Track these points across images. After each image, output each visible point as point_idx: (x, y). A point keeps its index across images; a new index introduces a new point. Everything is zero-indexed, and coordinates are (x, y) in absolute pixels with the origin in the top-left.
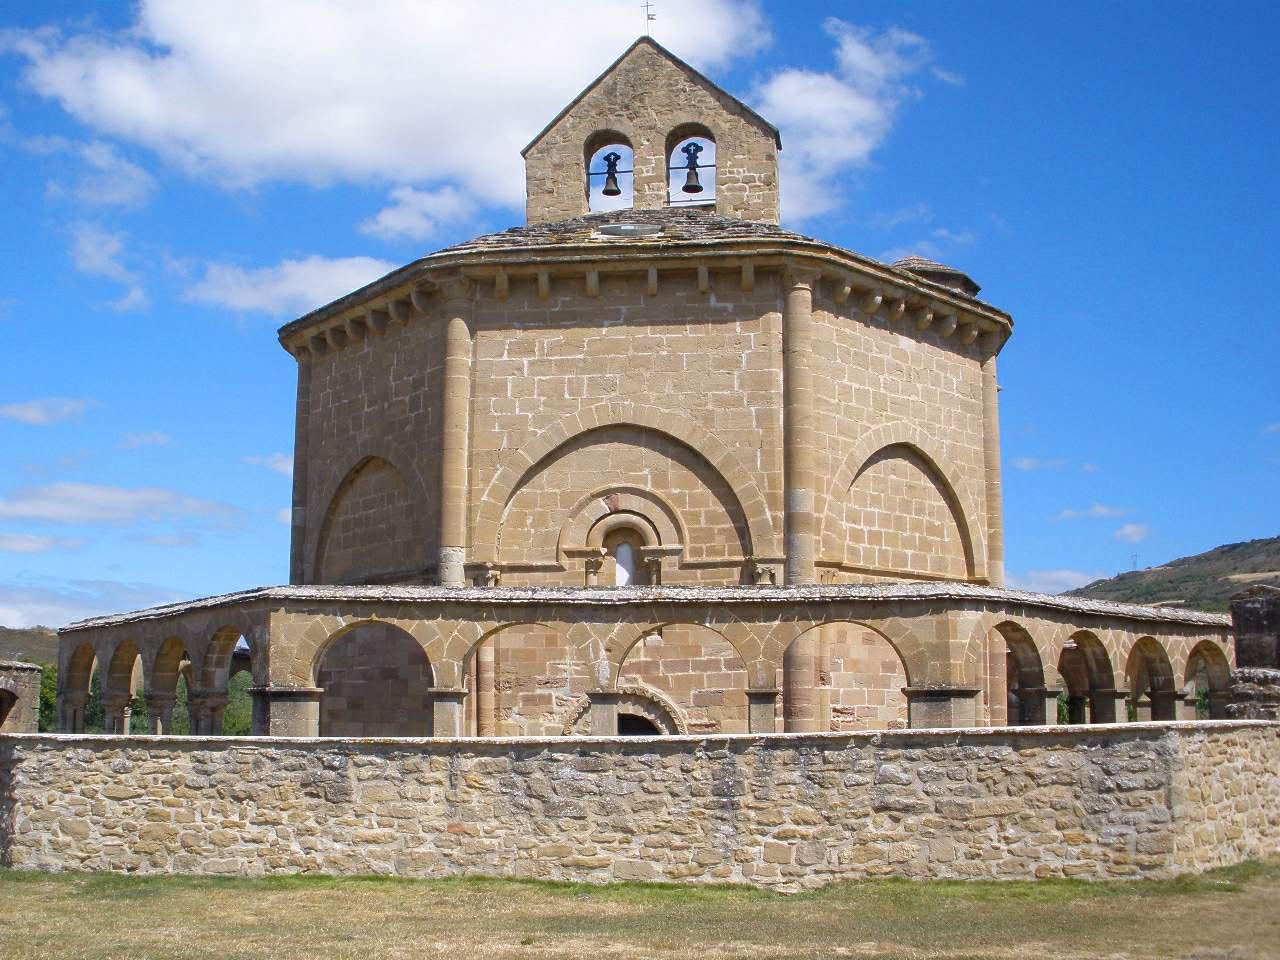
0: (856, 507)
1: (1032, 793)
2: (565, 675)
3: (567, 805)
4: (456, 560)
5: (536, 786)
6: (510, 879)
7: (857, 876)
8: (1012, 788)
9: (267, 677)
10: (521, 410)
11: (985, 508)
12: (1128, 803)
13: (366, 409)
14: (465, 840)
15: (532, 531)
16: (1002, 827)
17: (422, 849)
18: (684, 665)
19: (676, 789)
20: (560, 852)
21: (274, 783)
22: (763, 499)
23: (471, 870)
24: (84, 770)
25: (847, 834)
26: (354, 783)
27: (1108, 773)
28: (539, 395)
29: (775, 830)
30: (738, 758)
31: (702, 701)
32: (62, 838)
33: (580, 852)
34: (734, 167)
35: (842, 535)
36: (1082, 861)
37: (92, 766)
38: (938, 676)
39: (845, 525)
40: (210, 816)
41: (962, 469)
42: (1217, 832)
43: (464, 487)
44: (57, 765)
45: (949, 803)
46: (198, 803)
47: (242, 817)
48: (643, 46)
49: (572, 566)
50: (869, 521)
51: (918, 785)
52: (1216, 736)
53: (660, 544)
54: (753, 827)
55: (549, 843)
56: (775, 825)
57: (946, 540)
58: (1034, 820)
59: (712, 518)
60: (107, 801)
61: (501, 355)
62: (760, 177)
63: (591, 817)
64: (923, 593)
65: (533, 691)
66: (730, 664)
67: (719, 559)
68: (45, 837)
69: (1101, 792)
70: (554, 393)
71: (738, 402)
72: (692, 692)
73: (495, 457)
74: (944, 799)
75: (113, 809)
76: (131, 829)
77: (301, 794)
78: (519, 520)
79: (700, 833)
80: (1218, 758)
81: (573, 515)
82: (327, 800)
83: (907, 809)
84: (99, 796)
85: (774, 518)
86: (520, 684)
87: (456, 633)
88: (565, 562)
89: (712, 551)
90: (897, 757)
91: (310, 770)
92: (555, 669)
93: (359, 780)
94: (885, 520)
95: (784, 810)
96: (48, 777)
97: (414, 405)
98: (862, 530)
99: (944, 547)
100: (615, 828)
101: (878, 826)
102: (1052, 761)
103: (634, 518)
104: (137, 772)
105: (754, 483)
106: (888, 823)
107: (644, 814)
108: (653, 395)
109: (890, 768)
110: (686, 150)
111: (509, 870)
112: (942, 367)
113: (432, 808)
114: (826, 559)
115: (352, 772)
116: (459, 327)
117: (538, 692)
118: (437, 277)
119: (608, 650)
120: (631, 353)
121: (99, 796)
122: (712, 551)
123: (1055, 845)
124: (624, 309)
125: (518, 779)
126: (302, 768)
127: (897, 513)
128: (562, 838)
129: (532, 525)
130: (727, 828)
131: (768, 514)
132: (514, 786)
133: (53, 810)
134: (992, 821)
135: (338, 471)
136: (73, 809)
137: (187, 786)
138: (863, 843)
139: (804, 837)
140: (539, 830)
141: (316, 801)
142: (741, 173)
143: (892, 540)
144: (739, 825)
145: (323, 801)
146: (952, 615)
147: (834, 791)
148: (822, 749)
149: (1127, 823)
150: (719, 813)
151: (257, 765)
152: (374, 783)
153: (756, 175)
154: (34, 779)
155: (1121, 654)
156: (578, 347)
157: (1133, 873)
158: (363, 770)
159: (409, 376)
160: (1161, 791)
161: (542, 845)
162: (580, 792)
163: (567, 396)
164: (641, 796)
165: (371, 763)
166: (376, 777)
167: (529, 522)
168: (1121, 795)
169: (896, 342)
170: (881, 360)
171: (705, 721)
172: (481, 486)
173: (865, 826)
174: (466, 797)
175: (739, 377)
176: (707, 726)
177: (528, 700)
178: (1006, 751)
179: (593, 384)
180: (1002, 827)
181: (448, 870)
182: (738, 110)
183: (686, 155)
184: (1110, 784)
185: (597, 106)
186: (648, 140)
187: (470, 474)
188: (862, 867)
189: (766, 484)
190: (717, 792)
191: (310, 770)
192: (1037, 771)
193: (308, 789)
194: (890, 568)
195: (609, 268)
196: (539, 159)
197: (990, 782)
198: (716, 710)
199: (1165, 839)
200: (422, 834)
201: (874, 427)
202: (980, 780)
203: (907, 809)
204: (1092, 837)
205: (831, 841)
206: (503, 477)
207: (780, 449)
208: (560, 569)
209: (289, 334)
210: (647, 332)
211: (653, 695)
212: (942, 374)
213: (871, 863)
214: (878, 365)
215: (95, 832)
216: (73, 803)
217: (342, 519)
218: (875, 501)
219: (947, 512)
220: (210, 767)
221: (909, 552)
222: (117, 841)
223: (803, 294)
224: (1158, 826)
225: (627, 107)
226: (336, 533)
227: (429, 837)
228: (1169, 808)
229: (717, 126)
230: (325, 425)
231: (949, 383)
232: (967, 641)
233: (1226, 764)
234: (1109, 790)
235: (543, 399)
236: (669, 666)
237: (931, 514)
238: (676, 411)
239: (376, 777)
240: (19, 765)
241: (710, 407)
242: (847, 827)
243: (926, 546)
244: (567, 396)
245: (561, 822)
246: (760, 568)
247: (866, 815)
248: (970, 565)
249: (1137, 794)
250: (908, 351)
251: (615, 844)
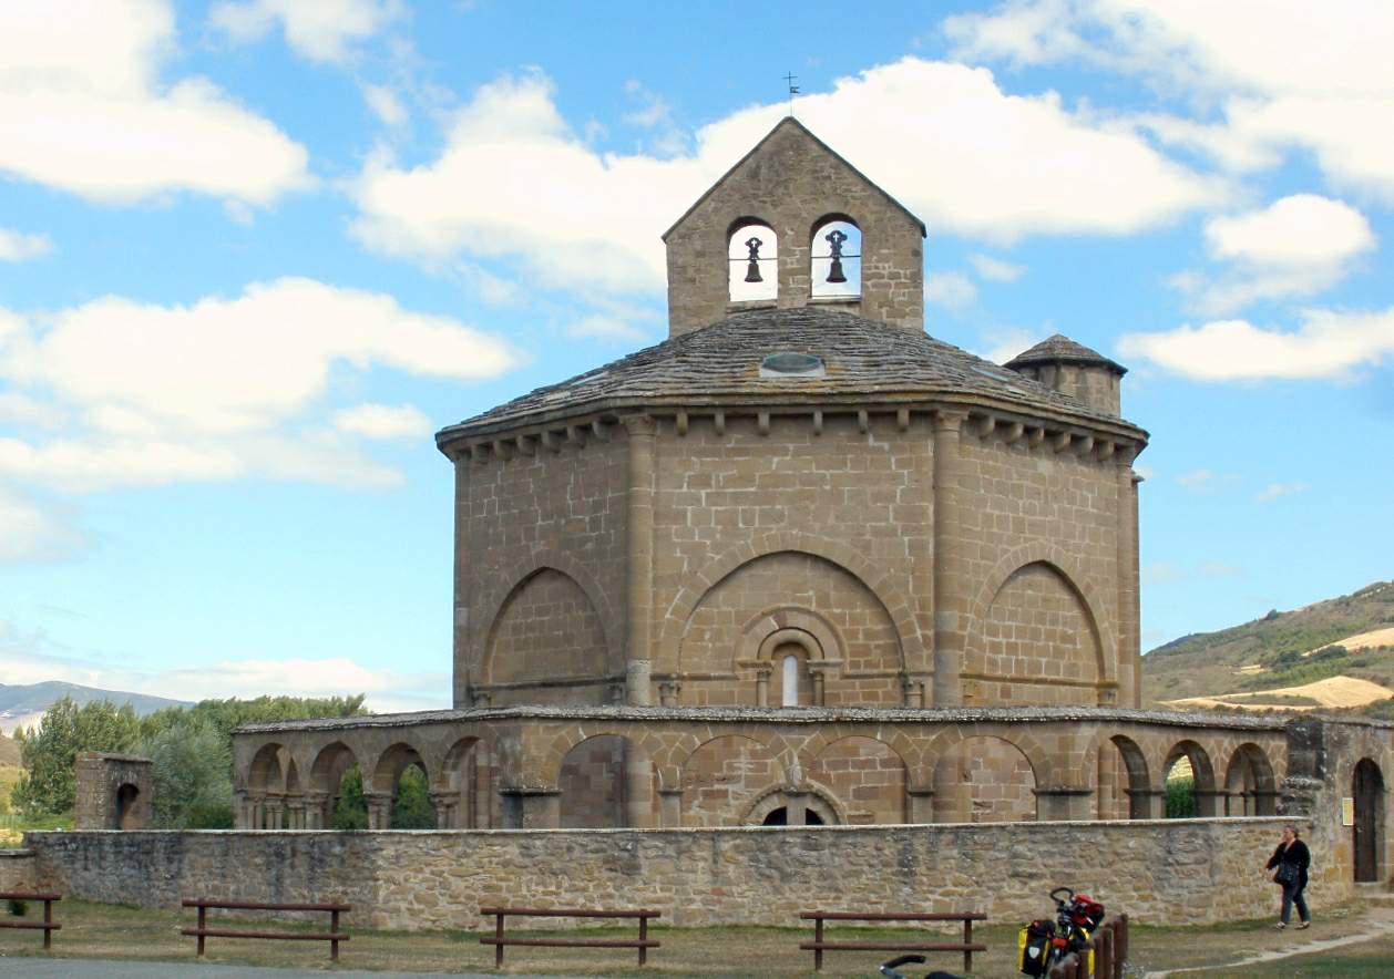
0: (996, 622)
1: (1119, 866)
2: (739, 772)
3: (797, 873)
4: (643, 670)
5: (775, 861)
6: (757, 926)
7: (997, 922)
8: (1104, 863)
10: (700, 537)
11: (1116, 615)
12: (1183, 873)
13: (540, 522)
14: (725, 899)
15: (710, 645)
16: (1096, 890)
17: (693, 907)
18: (845, 764)
19: (875, 862)
20: (791, 906)
21: (582, 862)
22: (913, 618)
23: (729, 921)
24: (433, 856)
25: (990, 893)
26: (642, 861)
27: (1170, 852)
28: (716, 524)
29: (940, 890)
30: (915, 841)
31: (859, 794)
32: (416, 906)
33: (806, 907)
34: (878, 261)
35: (982, 647)
36: (1152, 913)
37: (439, 854)
38: (1060, 781)
39: (986, 639)
40: (533, 887)
41: (1095, 580)
42: (1250, 895)
43: (650, 606)
44: (411, 853)
45: (1059, 873)
46: (524, 878)
47: (559, 887)
48: (787, 126)
49: (746, 676)
50: (1007, 635)
51: (1039, 860)
52: (1252, 827)
53: (824, 657)
54: (925, 888)
55: (784, 901)
56: (940, 886)
57: (1079, 647)
58: (1119, 885)
59: (869, 635)
60: (452, 879)
61: (681, 487)
62: (905, 274)
63: (814, 882)
64: (1049, 715)
65: (712, 786)
66: (884, 763)
67: (875, 671)
68: (403, 906)
69: (1165, 865)
70: (729, 522)
71: (892, 532)
72: (852, 787)
73: (677, 579)
74: (1058, 869)
75: (458, 885)
76: (470, 898)
77: (603, 870)
78: (700, 635)
79: (889, 892)
80: (1253, 843)
81: (746, 631)
82: (623, 873)
83: (1031, 876)
84: (445, 875)
85: (924, 636)
86: (700, 781)
87: (678, 744)
88: (740, 673)
89: (868, 664)
90: (1024, 841)
91: (609, 852)
92: (730, 767)
93: (647, 858)
94: (1021, 633)
95: (947, 877)
96: (404, 862)
97: (595, 523)
98: (1000, 643)
99: (1076, 653)
100: (830, 889)
101: (1015, 887)
102: (1132, 844)
103: (801, 634)
104: (475, 857)
105: (905, 605)
106: (1018, 885)
107: (851, 879)
108: (817, 526)
109: (1020, 848)
110: (830, 238)
111: (756, 920)
112: (1077, 485)
113: (700, 879)
114: (968, 672)
115: (641, 853)
116: (643, 458)
117: (717, 787)
118: (621, 414)
119: (799, 758)
120: (798, 487)
121: (445, 875)
122: (868, 664)
123: (1133, 902)
124: (791, 446)
125: (761, 856)
126: (603, 851)
127: (1033, 625)
128: (793, 897)
129: (710, 640)
130: (907, 889)
131: (919, 633)
132: (758, 861)
133: (409, 885)
134: (1090, 885)
135: (509, 579)
136: (425, 885)
137: (516, 866)
138: (1001, 898)
139: (961, 895)
140: (777, 891)
141: (614, 873)
142: (887, 268)
143: (1028, 649)
144: (916, 887)
145: (620, 874)
146: (1070, 732)
147: (981, 864)
148: (973, 833)
149: (1182, 887)
150: (902, 879)
151: (570, 849)
152: (657, 860)
153: (902, 272)
154: (393, 863)
155: (1222, 759)
156: (750, 481)
157: (1186, 920)
158: (649, 852)
159: (588, 497)
160: (1207, 866)
161: (779, 902)
162: (805, 864)
163: (741, 525)
164: (847, 867)
165: (656, 847)
166: (657, 856)
167: (707, 636)
168: (1178, 868)
169: (1035, 467)
170: (1021, 486)
171: (863, 812)
172: (664, 605)
173: (1002, 887)
174: (725, 869)
175: (895, 510)
176: (865, 816)
177: (707, 795)
178: (1100, 837)
179: (764, 514)
180: (1096, 890)
181: (712, 921)
182: (885, 201)
183: (830, 243)
184: (1170, 860)
185: (739, 190)
186: (792, 230)
187: (656, 596)
188: (1001, 916)
189: (917, 607)
190: (901, 864)
191: (609, 852)
192: (1120, 851)
193: (608, 866)
194: (1026, 675)
195: (780, 411)
196: (680, 244)
197: (1089, 858)
198: (872, 804)
199: (1208, 898)
200: (692, 896)
201: (1012, 549)
202: (1081, 857)
203: (1031, 876)
204: (1156, 894)
205: (978, 897)
206: (685, 598)
207: (930, 575)
208: (736, 678)
209: (452, 442)
211: (818, 790)
212: (1078, 492)
213: (1006, 913)
214: (1017, 490)
215: (443, 903)
216: (425, 880)
217: (511, 622)
218: (1013, 615)
219: (1081, 621)
220: (533, 852)
221: (1044, 660)
222: (460, 908)
223: (952, 428)
224: (1203, 889)
225: (771, 194)
226: (504, 635)
227: (698, 898)
228: (1211, 876)
229: (863, 217)
230: (491, 531)
231: (1084, 499)
232: (1084, 752)
233: (1260, 848)
234: (1170, 864)
235: (719, 527)
236: (834, 765)
237: (1065, 624)
238: (839, 540)
239: (657, 856)
240: (380, 853)
241: (868, 537)
242: (989, 888)
243: (1058, 653)
244: (741, 525)
245: (793, 885)
246: (911, 680)
247: (1004, 880)
248: (1102, 670)
249: (1189, 867)
250: (1046, 474)
251: (830, 901)
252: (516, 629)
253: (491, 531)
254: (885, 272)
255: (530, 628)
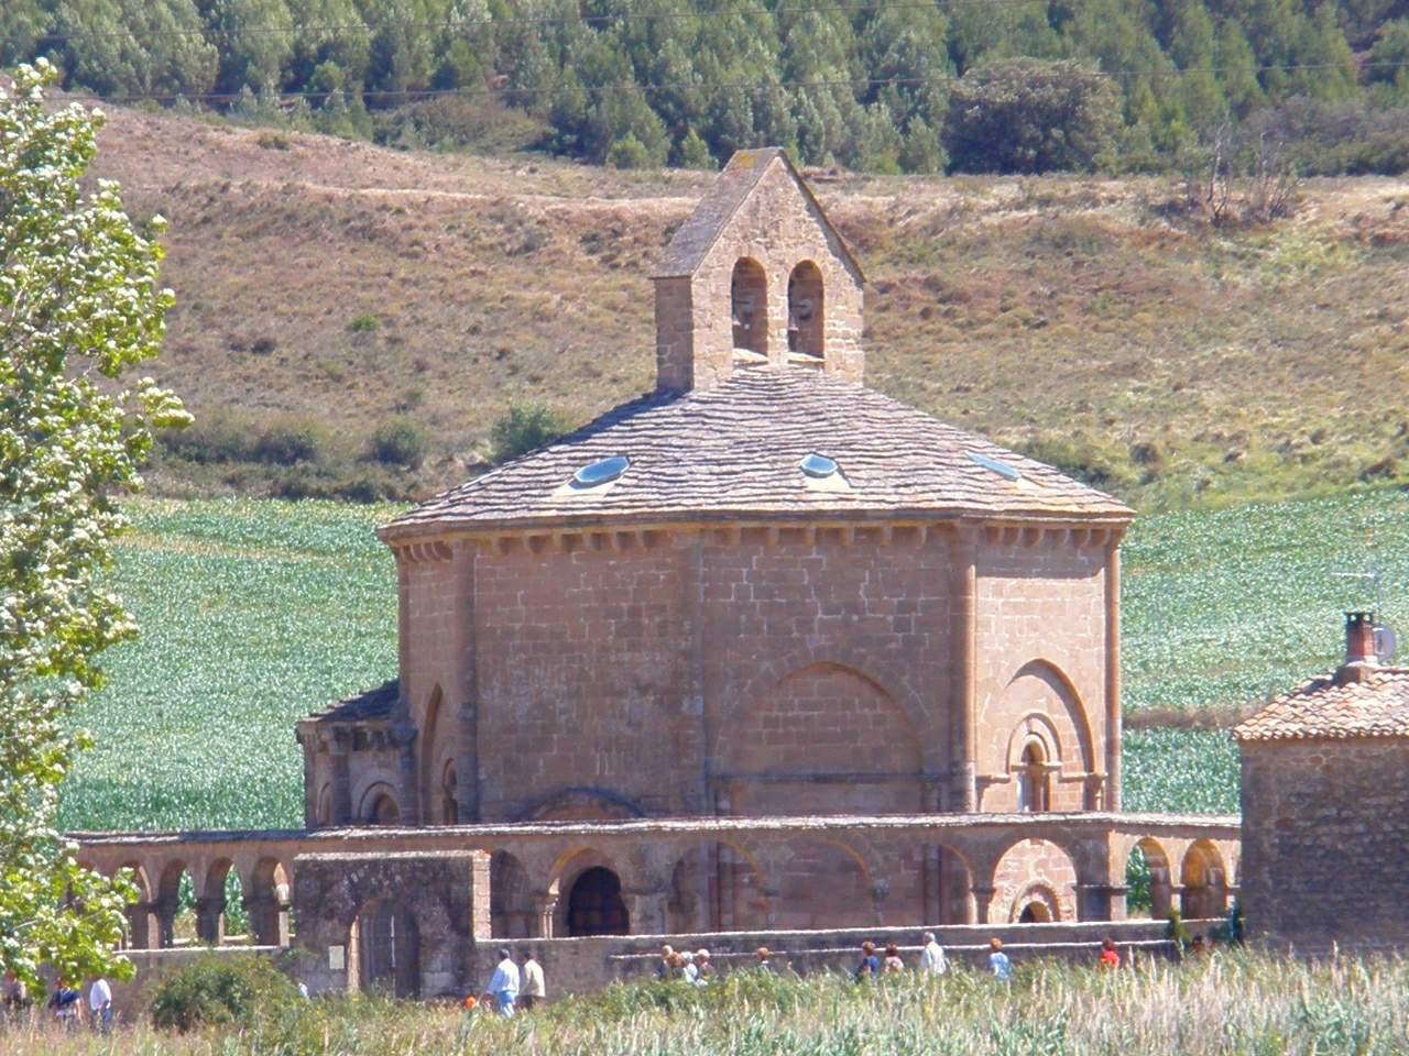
9: (1107, 878)
97: (901, 625)
124: (1041, 558)
210: (1052, 582)
252: (768, 722)
253: (743, 618)
254: (840, 331)
255: (795, 721)
